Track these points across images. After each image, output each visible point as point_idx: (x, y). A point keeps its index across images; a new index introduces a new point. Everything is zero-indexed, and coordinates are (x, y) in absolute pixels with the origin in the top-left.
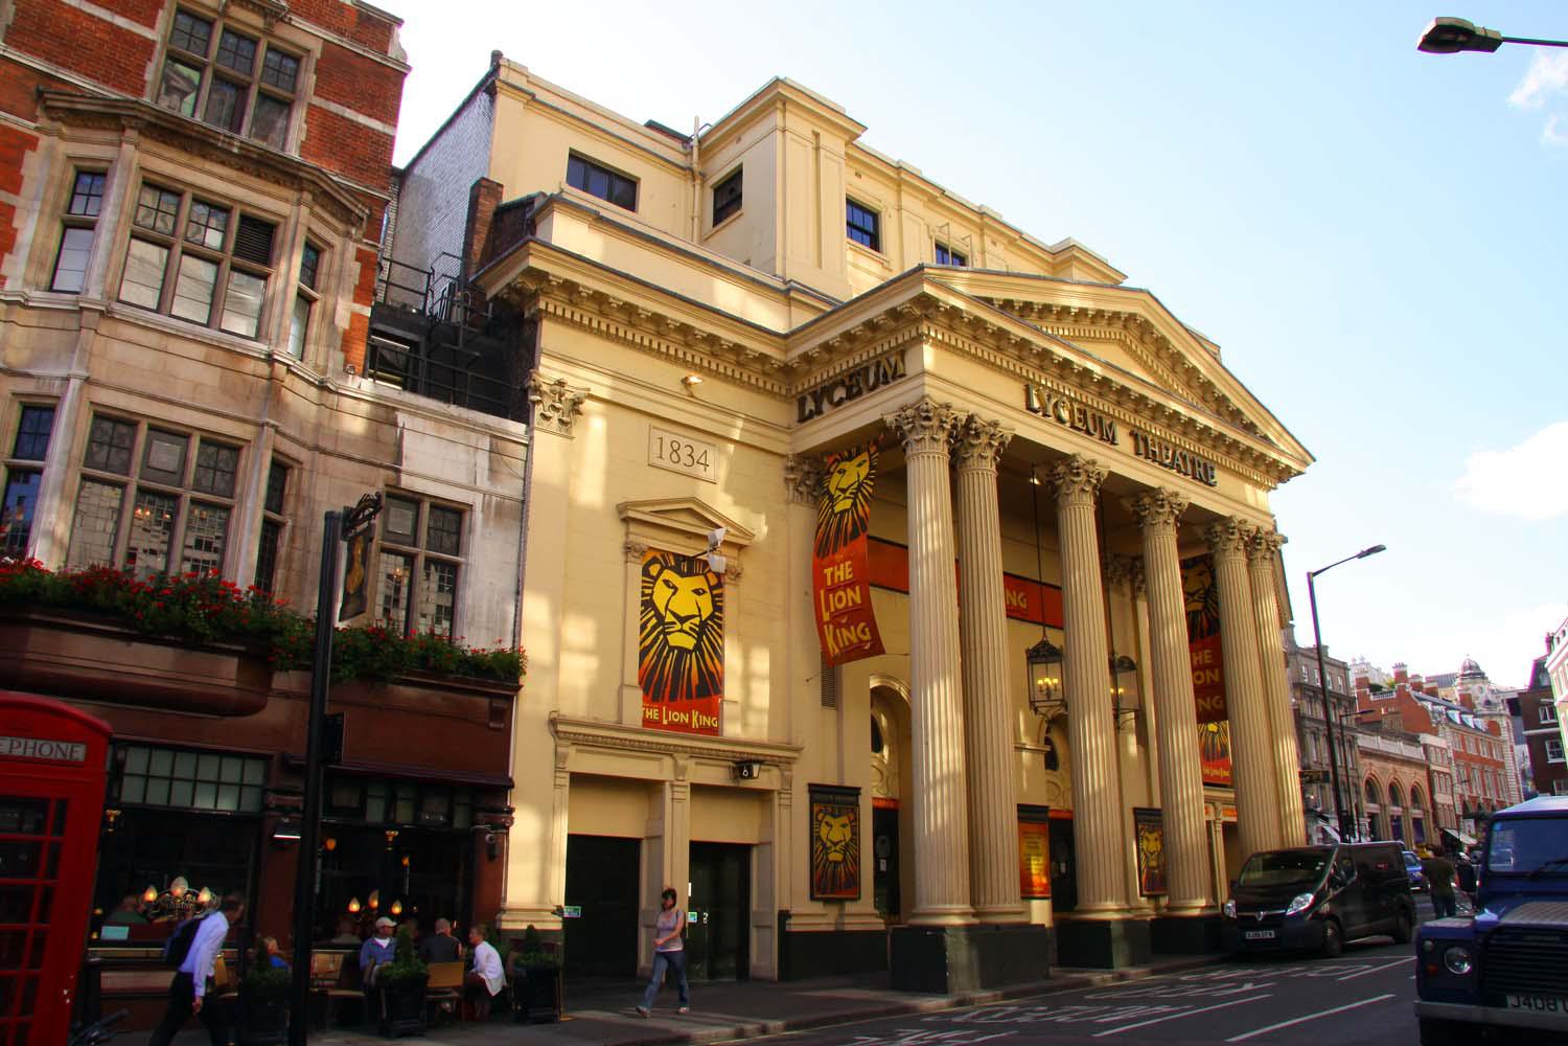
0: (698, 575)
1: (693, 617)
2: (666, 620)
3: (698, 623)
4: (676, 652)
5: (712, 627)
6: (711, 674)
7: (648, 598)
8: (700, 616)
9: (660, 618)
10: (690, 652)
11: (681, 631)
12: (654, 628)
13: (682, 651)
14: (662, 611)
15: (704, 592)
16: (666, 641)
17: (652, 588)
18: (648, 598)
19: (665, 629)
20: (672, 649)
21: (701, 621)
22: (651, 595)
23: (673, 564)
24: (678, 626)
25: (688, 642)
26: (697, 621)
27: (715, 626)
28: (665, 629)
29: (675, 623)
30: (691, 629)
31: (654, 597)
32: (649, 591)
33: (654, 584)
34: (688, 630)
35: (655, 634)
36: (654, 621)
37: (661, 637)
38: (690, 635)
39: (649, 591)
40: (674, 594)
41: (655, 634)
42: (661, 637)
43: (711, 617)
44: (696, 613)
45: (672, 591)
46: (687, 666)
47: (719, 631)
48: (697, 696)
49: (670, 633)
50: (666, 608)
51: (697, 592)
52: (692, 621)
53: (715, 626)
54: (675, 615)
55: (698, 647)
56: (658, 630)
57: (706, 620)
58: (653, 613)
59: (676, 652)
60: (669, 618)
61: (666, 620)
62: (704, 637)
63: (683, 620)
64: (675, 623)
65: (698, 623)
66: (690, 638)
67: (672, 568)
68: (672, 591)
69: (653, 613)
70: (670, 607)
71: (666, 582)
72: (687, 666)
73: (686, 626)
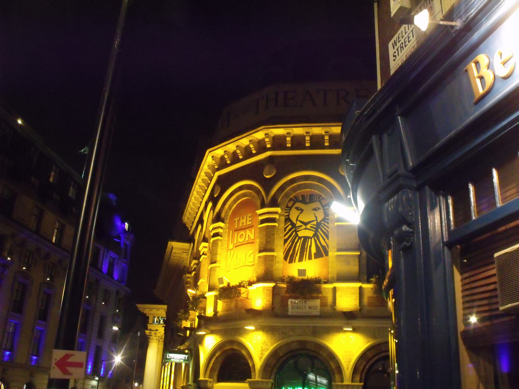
0: (316, 201)
1: (314, 221)
2: (297, 225)
3: (315, 224)
4: (302, 239)
5: (324, 224)
6: (323, 247)
7: (287, 217)
8: (317, 220)
9: (293, 225)
10: (311, 238)
11: (306, 229)
12: (290, 230)
13: (306, 238)
14: (294, 221)
15: (319, 209)
16: (297, 235)
17: (289, 212)
18: (287, 217)
19: (296, 229)
20: (300, 238)
21: (317, 223)
22: (288, 216)
23: (301, 199)
24: (304, 227)
25: (310, 234)
26: (315, 223)
27: (326, 224)
28: (296, 229)
29: (302, 226)
30: (311, 227)
31: (290, 216)
32: (287, 214)
33: (290, 210)
34: (309, 228)
35: (291, 232)
36: (290, 227)
37: (294, 233)
38: (310, 229)
39: (287, 214)
40: (301, 213)
41: (291, 232)
42: (294, 233)
43: (324, 220)
44: (315, 219)
45: (301, 211)
46: (309, 244)
47: (328, 225)
48: (315, 258)
49: (299, 231)
50: (297, 220)
51: (315, 209)
52: (312, 223)
53: (326, 224)
54: (300, 221)
55: (316, 235)
56: (293, 230)
57: (320, 222)
58: (289, 223)
59: (302, 239)
60: (299, 224)
61: (297, 225)
62: (319, 230)
63: (306, 224)
64: (302, 226)
65: (315, 224)
66: (311, 231)
67: (300, 202)
68: (301, 211)
69: (289, 223)
70: (298, 219)
71: (297, 209)
72: (309, 244)
73: (308, 226)
